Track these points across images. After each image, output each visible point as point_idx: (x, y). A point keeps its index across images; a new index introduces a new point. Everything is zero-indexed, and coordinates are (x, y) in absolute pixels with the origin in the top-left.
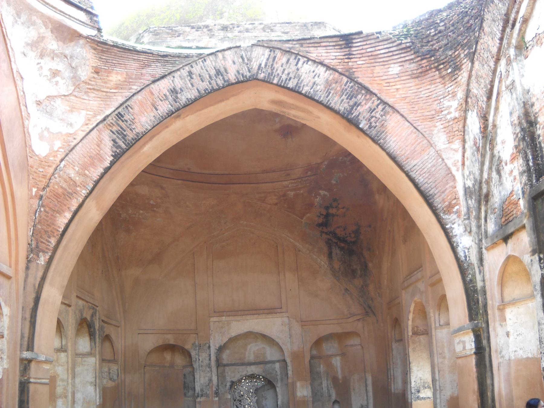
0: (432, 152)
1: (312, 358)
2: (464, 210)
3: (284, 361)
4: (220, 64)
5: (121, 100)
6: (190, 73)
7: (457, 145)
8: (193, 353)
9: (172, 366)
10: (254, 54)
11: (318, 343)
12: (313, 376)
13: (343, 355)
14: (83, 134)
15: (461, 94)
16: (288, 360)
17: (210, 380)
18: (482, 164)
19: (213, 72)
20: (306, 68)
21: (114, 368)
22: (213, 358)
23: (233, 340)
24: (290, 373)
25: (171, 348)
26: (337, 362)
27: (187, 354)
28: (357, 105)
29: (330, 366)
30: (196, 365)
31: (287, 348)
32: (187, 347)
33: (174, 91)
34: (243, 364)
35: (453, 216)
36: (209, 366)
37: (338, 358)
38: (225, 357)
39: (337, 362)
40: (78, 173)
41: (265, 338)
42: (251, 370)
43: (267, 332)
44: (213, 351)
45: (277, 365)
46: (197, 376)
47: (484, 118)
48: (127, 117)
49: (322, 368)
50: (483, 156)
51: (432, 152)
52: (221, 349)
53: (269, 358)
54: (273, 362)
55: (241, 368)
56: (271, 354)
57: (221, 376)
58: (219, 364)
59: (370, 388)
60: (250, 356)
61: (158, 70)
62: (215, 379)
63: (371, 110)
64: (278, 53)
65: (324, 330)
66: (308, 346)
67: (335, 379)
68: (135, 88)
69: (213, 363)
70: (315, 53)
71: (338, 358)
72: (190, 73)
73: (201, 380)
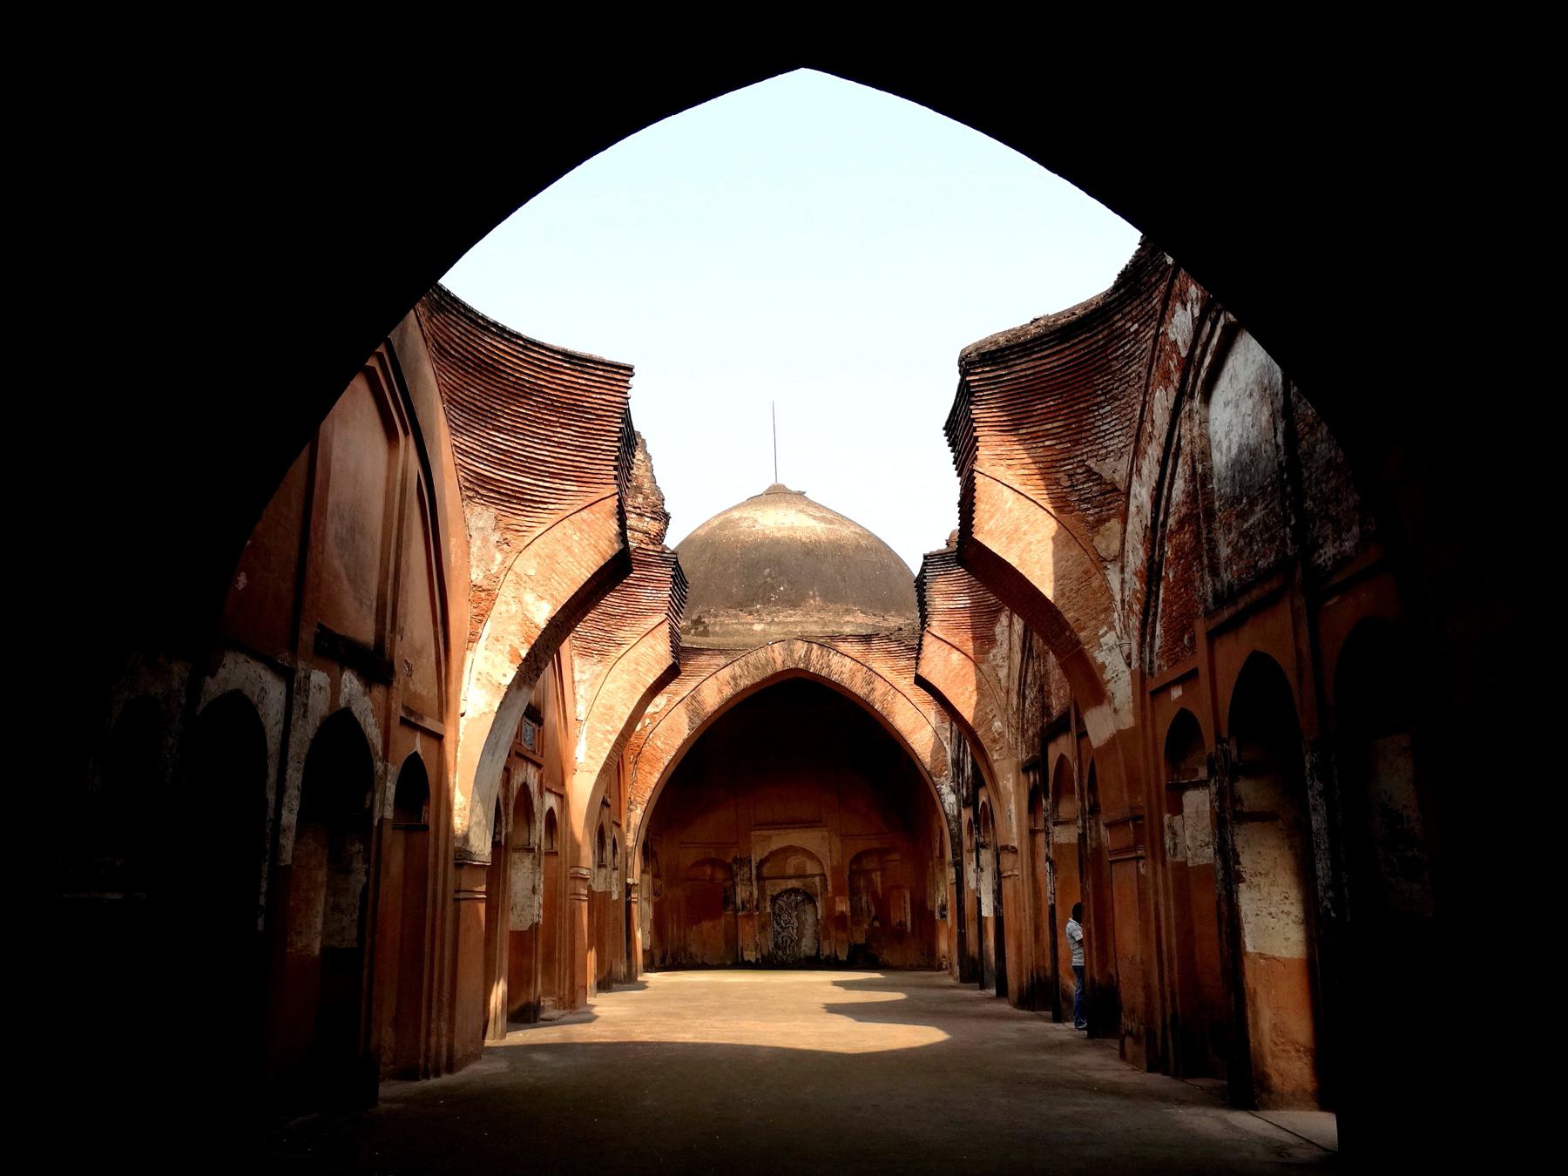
1: (852, 872)
3: (823, 875)
6: (747, 664)
9: (712, 879)
11: (857, 859)
12: (854, 893)
13: (883, 870)
16: (828, 874)
20: (835, 659)
21: (659, 883)
23: (772, 854)
24: (830, 888)
25: (713, 863)
26: (877, 877)
29: (870, 882)
31: (827, 863)
33: (734, 678)
38: (765, 871)
42: (792, 884)
49: (862, 883)
53: (809, 872)
54: (813, 876)
56: (811, 868)
57: (762, 890)
58: (760, 878)
60: (790, 871)
61: (722, 660)
62: (756, 892)
63: (885, 694)
65: (861, 846)
66: (847, 861)
67: (874, 894)
68: (706, 675)
70: (843, 647)
73: (741, 893)
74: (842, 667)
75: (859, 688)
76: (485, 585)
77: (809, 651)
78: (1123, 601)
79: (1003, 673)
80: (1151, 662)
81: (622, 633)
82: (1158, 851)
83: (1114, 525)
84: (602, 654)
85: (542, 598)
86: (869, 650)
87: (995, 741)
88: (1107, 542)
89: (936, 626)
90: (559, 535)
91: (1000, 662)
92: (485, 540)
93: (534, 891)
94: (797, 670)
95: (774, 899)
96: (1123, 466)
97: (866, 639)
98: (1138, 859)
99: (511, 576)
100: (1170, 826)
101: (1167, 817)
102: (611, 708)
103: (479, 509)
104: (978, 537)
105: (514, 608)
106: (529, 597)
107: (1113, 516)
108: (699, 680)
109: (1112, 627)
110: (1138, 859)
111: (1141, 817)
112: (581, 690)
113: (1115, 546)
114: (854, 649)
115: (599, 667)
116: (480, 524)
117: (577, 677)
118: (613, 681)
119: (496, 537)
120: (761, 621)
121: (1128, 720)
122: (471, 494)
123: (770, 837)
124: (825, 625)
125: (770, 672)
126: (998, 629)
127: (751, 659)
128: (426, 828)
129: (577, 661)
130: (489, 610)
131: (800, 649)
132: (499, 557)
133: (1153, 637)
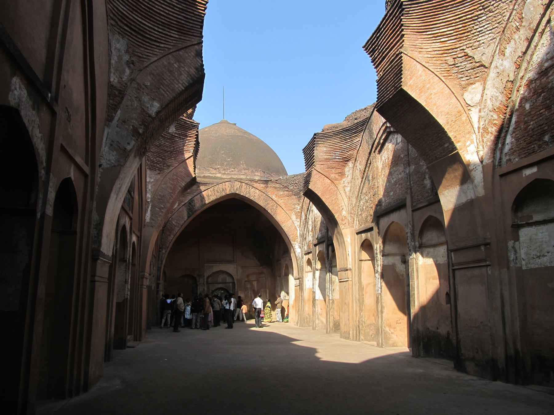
0: (291, 221)
2: (299, 240)
4: (224, 187)
5: (190, 198)
6: (214, 190)
7: (299, 220)
8: (197, 278)
10: (235, 184)
13: (258, 281)
14: (177, 209)
15: (300, 205)
16: (236, 282)
17: (204, 289)
18: (305, 229)
19: (221, 190)
22: (205, 281)
23: (214, 273)
26: (255, 283)
27: (194, 279)
28: (268, 204)
30: (198, 283)
32: (195, 276)
34: (217, 283)
35: (296, 242)
36: (204, 284)
37: (256, 282)
38: (210, 280)
39: (255, 283)
40: (176, 222)
41: (230, 275)
42: (220, 286)
43: (228, 271)
44: (205, 277)
45: (231, 284)
46: (198, 288)
47: (306, 216)
48: (192, 204)
49: (249, 286)
50: (305, 226)
51: (291, 221)
52: (208, 277)
54: (230, 283)
55: (216, 285)
56: (228, 279)
57: (208, 288)
58: (207, 283)
59: (268, 295)
60: (220, 280)
62: (206, 289)
63: (273, 206)
64: (244, 184)
69: (205, 283)
70: (256, 185)
71: (256, 282)
72: (214, 190)
74: (254, 194)
75: (261, 203)
76: (118, 86)
77: (241, 186)
78: (479, 128)
79: (348, 189)
80: (500, 159)
81: (170, 161)
82: (503, 261)
83: (478, 86)
84: (161, 170)
85: (154, 99)
86: (267, 187)
87: (342, 220)
88: (473, 94)
89: (318, 166)
90: (165, 63)
91: (347, 185)
92: (120, 58)
93: (126, 282)
94: (236, 194)
95: (213, 292)
96: (489, 51)
97: (266, 182)
98: (487, 266)
99: (134, 85)
100: (513, 247)
101: (511, 243)
102: (163, 196)
103: (117, 36)
104: (405, 88)
105: (136, 104)
106: (145, 98)
107: (478, 81)
108: (193, 196)
109: (472, 142)
110: (487, 266)
111: (489, 244)
112: (149, 187)
113: (478, 97)
114: (261, 186)
115: (159, 176)
116: (118, 46)
117: (148, 180)
118: (165, 184)
119: (126, 58)
120: (220, 173)
121: (481, 192)
122: (113, 23)
123: (213, 266)
124: (247, 176)
125: (224, 194)
126: (347, 169)
127: (216, 188)
128: (75, 233)
129: (148, 172)
130: (120, 103)
131: (237, 184)
132: (128, 71)
133: (503, 144)
